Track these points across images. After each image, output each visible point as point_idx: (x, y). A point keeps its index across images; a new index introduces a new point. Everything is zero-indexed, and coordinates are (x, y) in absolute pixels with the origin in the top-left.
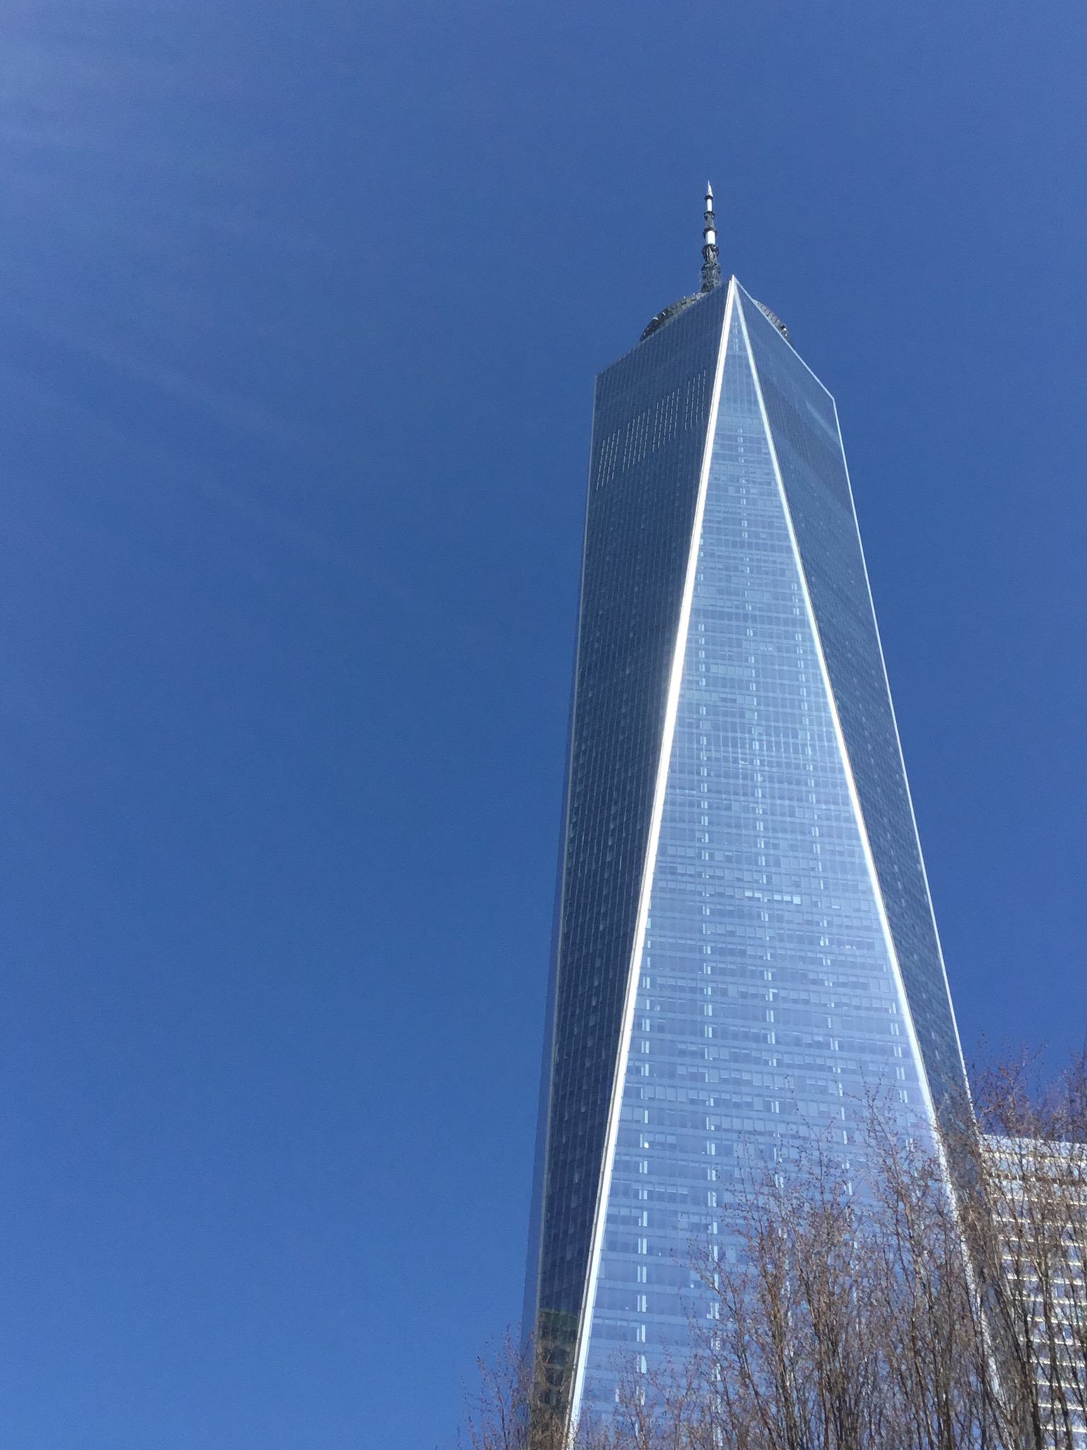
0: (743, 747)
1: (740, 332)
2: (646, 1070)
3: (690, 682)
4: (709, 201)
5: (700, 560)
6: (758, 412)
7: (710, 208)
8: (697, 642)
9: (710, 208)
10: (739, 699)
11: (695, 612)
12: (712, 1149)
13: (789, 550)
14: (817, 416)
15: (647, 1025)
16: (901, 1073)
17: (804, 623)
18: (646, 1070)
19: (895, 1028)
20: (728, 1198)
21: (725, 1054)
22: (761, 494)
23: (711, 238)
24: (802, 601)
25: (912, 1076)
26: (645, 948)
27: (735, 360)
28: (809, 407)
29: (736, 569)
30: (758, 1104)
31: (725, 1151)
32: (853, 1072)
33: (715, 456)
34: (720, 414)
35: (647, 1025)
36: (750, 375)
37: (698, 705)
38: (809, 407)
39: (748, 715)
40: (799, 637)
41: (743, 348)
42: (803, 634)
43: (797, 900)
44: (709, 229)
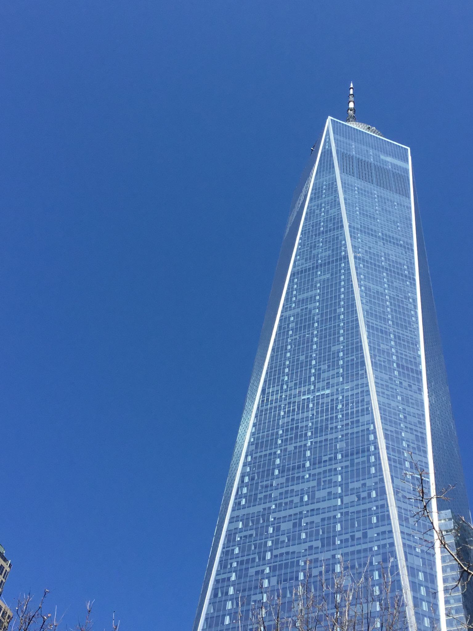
0: (309, 327)
2: (243, 502)
3: (287, 308)
4: (351, 90)
8: (293, 288)
10: (309, 306)
11: (293, 275)
12: (271, 530)
13: (342, 226)
14: (389, 159)
15: (246, 479)
16: (372, 459)
17: (346, 257)
18: (243, 502)
19: (372, 437)
20: (276, 552)
21: (283, 480)
22: (331, 207)
23: (351, 105)
24: (346, 247)
28: (382, 157)
29: (315, 246)
30: (296, 500)
31: (277, 529)
32: (347, 467)
33: (311, 199)
35: (246, 479)
36: (332, 156)
37: (289, 317)
38: (382, 157)
39: (313, 312)
40: (343, 265)
42: (344, 263)
43: (327, 392)
44: (350, 102)
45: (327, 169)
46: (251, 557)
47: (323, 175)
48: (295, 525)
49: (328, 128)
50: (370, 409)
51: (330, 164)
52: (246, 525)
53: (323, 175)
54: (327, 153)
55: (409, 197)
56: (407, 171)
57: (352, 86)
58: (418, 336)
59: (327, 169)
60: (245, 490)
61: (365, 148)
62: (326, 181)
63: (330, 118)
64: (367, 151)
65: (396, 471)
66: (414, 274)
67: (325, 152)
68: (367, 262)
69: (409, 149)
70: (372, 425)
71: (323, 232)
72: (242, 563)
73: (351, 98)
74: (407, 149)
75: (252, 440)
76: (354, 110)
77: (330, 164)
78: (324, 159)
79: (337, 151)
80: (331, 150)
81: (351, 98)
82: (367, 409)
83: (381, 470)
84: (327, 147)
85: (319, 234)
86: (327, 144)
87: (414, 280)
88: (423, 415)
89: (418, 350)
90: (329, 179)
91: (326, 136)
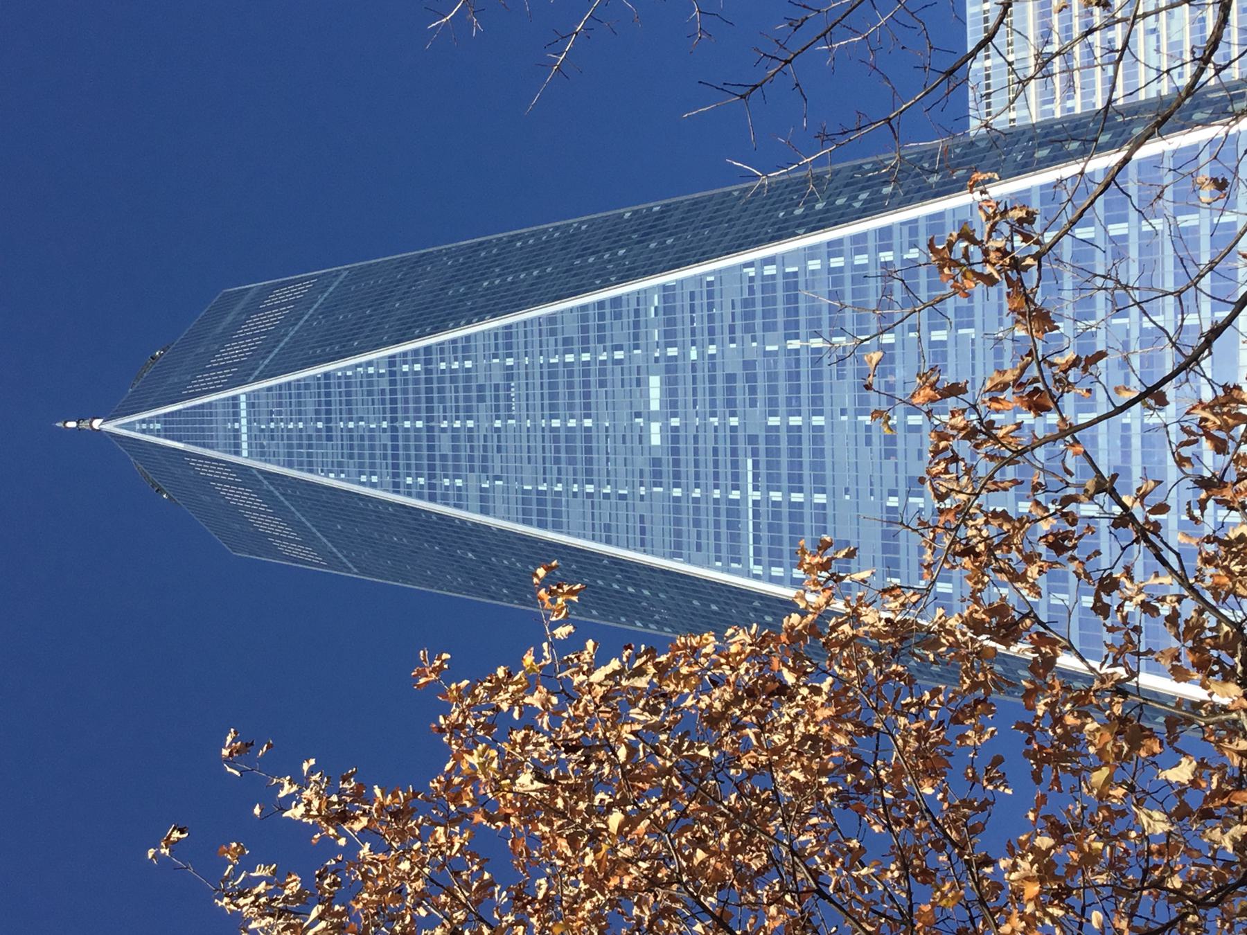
1: (143, 421)
6: (210, 404)
11: (396, 488)
13: (327, 375)
14: (230, 318)
16: (815, 265)
17: (392, 361)
19: (770, 270)
25: (812, 252)
26: (722, 570)
27: (170, 426)
36: (180, 411)
38: (219, 330)
40: (405, 368)
41: (157, 419)
45: (203, 422)
47: (211, 430)
49: (121, 426)
50: (710, 279)
51: (195, 414)
53: (211, 430)
54: (170, 426)
57: (60, 425)
59: (203, 422)
62: (225, 422)
67: (166, 430)
70: (745, 270)
71: (328, 421)
73: (85, 425)
74: (224, 296)
75: (719, 564)
77: (195, 414)
78: (179, 430)
80: (165, 415)
81: (85, 425)
82: (710, 284)
83: (839, 242)
84: (158, 426)
85: (329, 429)
86: (152, 426)
87: (481, 244)
90: (224, 414)
91: (134, 430)
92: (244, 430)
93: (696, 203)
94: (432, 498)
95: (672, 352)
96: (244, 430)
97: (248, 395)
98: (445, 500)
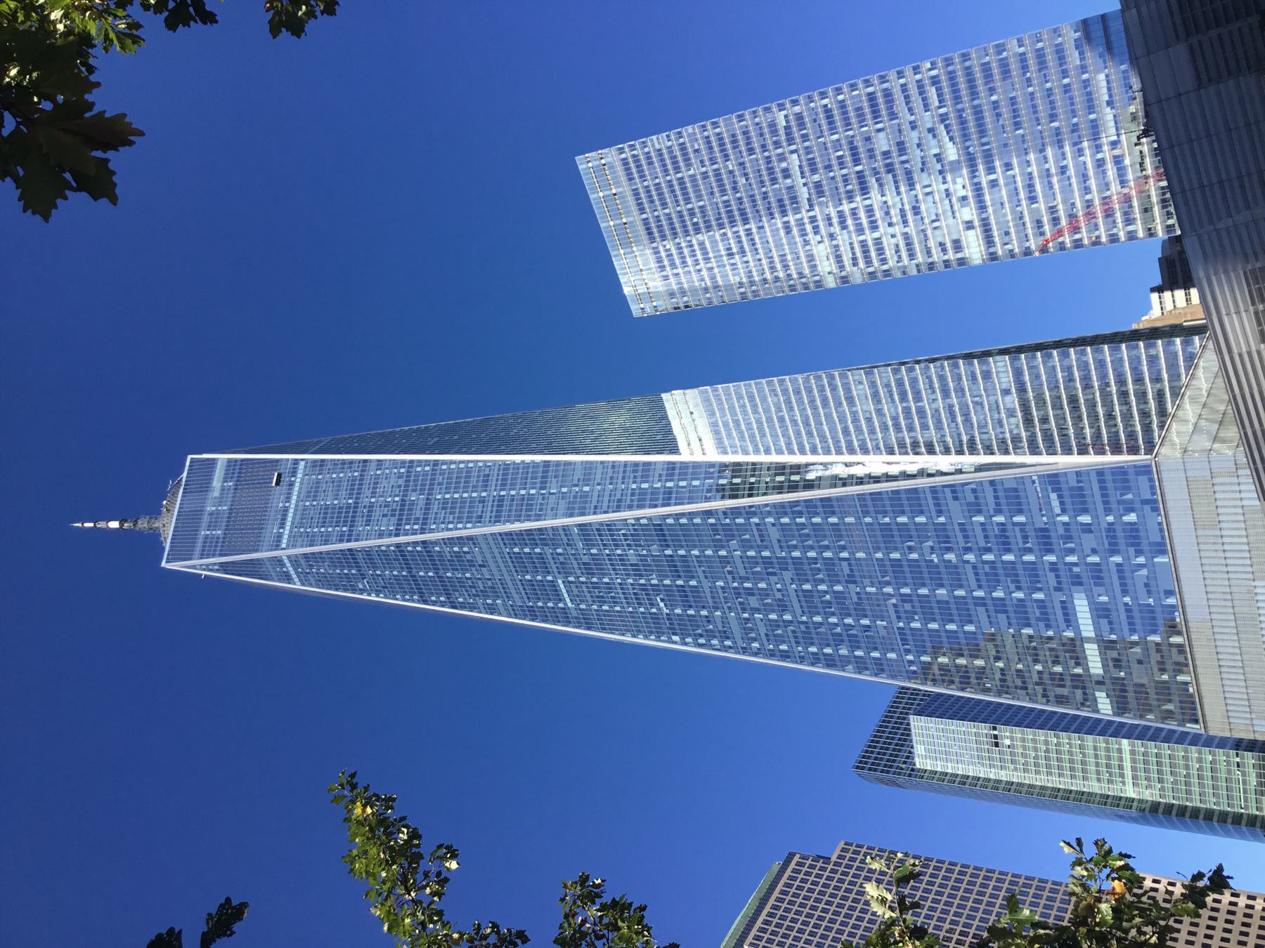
4: (86, 525)
5: (386, 597)
6: (258, 560)
7: (91, 525)
9: (91, 525)
11: (425, 602)
13: (350, 550)
14: (217, 483)
15: (702, 641)
16: (670, 521)
17: (398, 546)
23: (114, 525)
31: (758, 610)
34: (273, 580)
35: (702, 641)
38: (216, 494)
46: (791, 635)
48: (753, 594)
52: (755, 640)
54: (224, 567)
55: (277, 461)
56: (229, 461)
58: (494, 462)
60: (715, 642)
61: (206, 518)
63: (163, 564)
64: (211, 514)
65: (681, 498)
66: (403, 462)
68: (400, 520)
69: (190, 457)
72: (797, 642)
73: (101, 525)
74: (192, 461)
76: (122, 522)
79: (221, 555)
81: (101, 525)
87: (411, 461)
88: (602, 462)
89: (514, 463)
92: (292, 572)
93: (567, 463)
94: (454, 607)
95: (594, 551)
96: (292, 572)
97: (289, 557)
98: (463, 608)
